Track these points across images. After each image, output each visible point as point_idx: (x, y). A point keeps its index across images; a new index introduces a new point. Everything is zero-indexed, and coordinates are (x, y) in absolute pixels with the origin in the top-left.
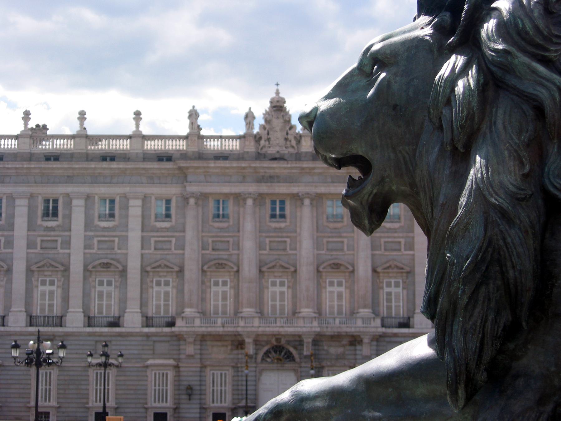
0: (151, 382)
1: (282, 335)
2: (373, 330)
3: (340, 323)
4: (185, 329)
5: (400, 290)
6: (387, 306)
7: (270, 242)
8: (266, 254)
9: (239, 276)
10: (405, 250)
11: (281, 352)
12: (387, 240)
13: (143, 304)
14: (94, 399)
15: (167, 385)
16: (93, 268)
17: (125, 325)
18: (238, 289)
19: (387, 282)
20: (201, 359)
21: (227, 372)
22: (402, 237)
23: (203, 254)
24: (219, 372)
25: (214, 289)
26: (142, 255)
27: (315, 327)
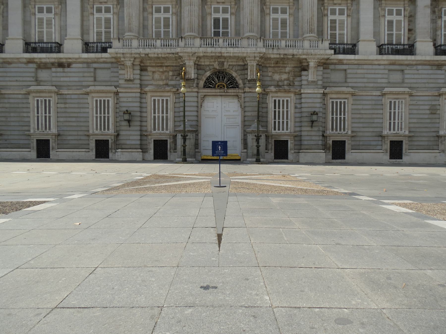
0: (93, 109)
1: (225, 58)
2: (322, 52)
3: (286, 46)
4: (121, 51)
5: (344, 17)
6: (331, 33)
11: (224, 78)
13: (84, 31)
14: (36, 127)
15: (108, 113)
17: (65, 51)
19: (331, 9)
20: (141, 85)
21: (168, 98)
24: (160, 99)
25: (155, 15)
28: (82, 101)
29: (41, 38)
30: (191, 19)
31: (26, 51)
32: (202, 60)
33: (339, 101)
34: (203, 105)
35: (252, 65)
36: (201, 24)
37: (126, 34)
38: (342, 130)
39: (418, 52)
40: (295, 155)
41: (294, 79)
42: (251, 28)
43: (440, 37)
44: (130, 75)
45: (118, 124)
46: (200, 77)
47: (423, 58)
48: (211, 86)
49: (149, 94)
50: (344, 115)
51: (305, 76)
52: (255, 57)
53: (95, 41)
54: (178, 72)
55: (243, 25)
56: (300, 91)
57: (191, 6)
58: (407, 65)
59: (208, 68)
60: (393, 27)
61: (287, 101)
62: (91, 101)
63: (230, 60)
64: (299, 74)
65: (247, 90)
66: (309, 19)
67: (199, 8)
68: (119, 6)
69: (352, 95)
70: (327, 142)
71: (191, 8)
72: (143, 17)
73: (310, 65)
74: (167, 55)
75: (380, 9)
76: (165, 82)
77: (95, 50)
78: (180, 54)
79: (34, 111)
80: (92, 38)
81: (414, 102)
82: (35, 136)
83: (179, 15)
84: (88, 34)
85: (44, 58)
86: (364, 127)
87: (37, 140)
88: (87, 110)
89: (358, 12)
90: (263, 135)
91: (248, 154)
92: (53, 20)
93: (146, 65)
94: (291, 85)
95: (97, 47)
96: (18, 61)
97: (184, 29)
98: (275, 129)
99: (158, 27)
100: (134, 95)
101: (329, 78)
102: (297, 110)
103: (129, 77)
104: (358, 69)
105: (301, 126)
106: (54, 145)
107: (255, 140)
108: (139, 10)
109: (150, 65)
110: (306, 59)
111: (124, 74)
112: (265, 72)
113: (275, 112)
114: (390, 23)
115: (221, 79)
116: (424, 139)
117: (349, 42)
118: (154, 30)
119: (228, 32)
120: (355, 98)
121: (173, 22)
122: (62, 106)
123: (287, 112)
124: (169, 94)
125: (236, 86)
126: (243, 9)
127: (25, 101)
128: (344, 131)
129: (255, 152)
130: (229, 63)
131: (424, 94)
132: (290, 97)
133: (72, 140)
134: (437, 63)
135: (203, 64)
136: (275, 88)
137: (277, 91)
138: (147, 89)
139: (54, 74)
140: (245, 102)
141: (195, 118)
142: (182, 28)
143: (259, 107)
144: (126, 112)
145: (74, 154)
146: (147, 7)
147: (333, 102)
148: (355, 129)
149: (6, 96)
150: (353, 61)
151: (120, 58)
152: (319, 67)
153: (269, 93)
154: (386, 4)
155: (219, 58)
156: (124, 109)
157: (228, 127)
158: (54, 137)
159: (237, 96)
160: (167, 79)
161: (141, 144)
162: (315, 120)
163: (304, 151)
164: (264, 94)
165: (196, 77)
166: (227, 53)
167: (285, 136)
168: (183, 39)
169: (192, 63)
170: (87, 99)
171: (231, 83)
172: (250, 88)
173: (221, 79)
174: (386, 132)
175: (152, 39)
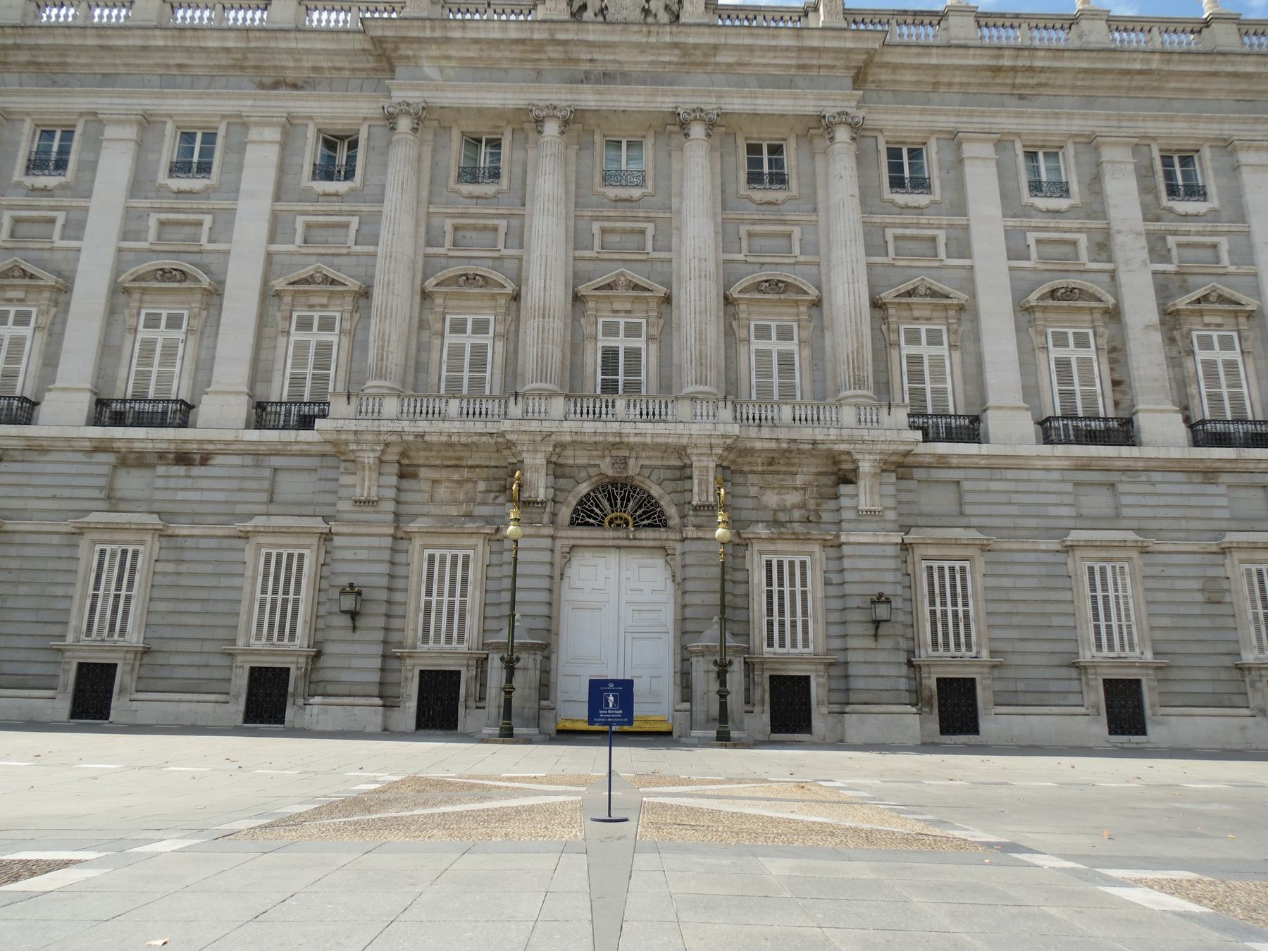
0: (254, 579)
1: (631, 447)
2: (890, 435)
3: (794, 420)
4: (352, 425)
5: (943, 350)
6: (910, 389)
7: (604, 231)
8: (591, 259)
9: (518, 309)
10: (948, 257)
11: (626, 500)
12: (900, 231)
13: (259, 371)
14: (84, 628)
15: (297, 592)
16: (135, 280)
17: (200, 423)
18: (516, 343)
21: (471, 553)
22: (939, 228)
23: (426, 256)
24: (449, 553)
25: (451, 339)
26: (269, 256)
27: (726, 425)
28: (227, 556)
29: (141, 390)
30: (543, 349)
31: (96, 420)
32: (569, 452)
33: (946, 565)
34: (568, 572)
35: (704, 466)
36: (568, 362)
37: (370, 383)
38: (963, 648)
39: (1145, 436)
40: (831, 719)
41: (818, 505)
42: (701, 372)
43: (1197, 401)
44: (369, 489)
45: (321, 624)
46: (560, 498)
47: (1163, 453)
48: (592, 521)
49: (417, 542)
50: (965, 604)
51: (848, 499)
52: (711, 448)
53: (285, 399)
54: (503, 483)
55: (680, 365)
56: (838, 536)
57: (544, 318)
58: (1124, 471)
59: (583, 474)
60: (1072, 376)
61: (803, 564)
62: (253, 557)
63: (644, 454)
64: (831, 491)
65: (690, 532)
66: (850, 351)
67: (565, 324)
68: (358, 315)
69: (982, 550)
70: (924, 682)
71: (544, 322)
72: (419, 343)
73: (861, 469)
74: (475, 439)
75: (1031, 331)
76: (464, 508)
77: (282, 423)
78: (509, 437)
79: (86, 582)
80: (278, 390)
81: (1156, 571)
82: (76, 654)
83: (512, 339)
84: (269, 381)
85: (142, 440)
86: (1023, 640)
87: (81, 665)
88: (236, 582)
89: (977, 337)
90: (738, 659)
91: (694, 717)
92: (181, 346)
93: (416, 462)
94: (810, 522)
95: (288, 413)
96: (69, 444)
97: (523, 374)
98: (771, 644)
99: (455, 367)
100: (375, 542)
101: (915, 503)
102: (833, 591)
103: (365, 495)
104: (991, 480)
105: (845, 636)
106: (127, 679)
107: (714, 675)
108: (410, 326)
109: (427, 462)
110: (849, 453)
111: (354, 486)
112: (739, 485)
113: (770, 594)
114: (1063, 365)
115: (619, 501)
116: (1200, 674)
117: (960, 412)
118: (444, 374)
119: (640, 383)
120: (989, 556)
121: (496, 355)
122: (170, 568)
123: (804, 594)
124: (472, 541)
125: (660, 521)
126: (679, 328)
127: (65, 552)
128: (967, 651)
129: (715, 709)
130: (641, 462)
131: (1181, 548)
132: (811, 554)
133: (183, 666)
134: (1201, 466)
135: (571, 462)
136: (768, 527)
137: (775, 536)
138: (413, 527)
139: (160, 483)
140: (684, 566)
141: (543, 610)
142: (519, 370)
143: (723, 580)
144: (348, 589)
145: (184, 707)
146: (431, 318)
147: (930, 569)
148: (999, 646)
149: (17, 538)
150: (976, 460)
151: (347, 443)
152: (885, 474)
153: (753, 541)
154: (1046, 320)
155: (617, 447)
156: (345, 581)
157: (635, 635)
158: (131, 656)
159: (664, 548)
160: (471, 500)
161: (381, 684)
162: (885, 618)
163: (858, 708)
164: (739, 545)
165: (550, 497)
166: (636, 434)
167: (801, 663)
168: (520, 399)
169: (540, 460)
170: (243, 550)
171: (647, 514)
172: (698, 527)
173: (619, 501)
174: (1088, 654)
175: (438, 397)
